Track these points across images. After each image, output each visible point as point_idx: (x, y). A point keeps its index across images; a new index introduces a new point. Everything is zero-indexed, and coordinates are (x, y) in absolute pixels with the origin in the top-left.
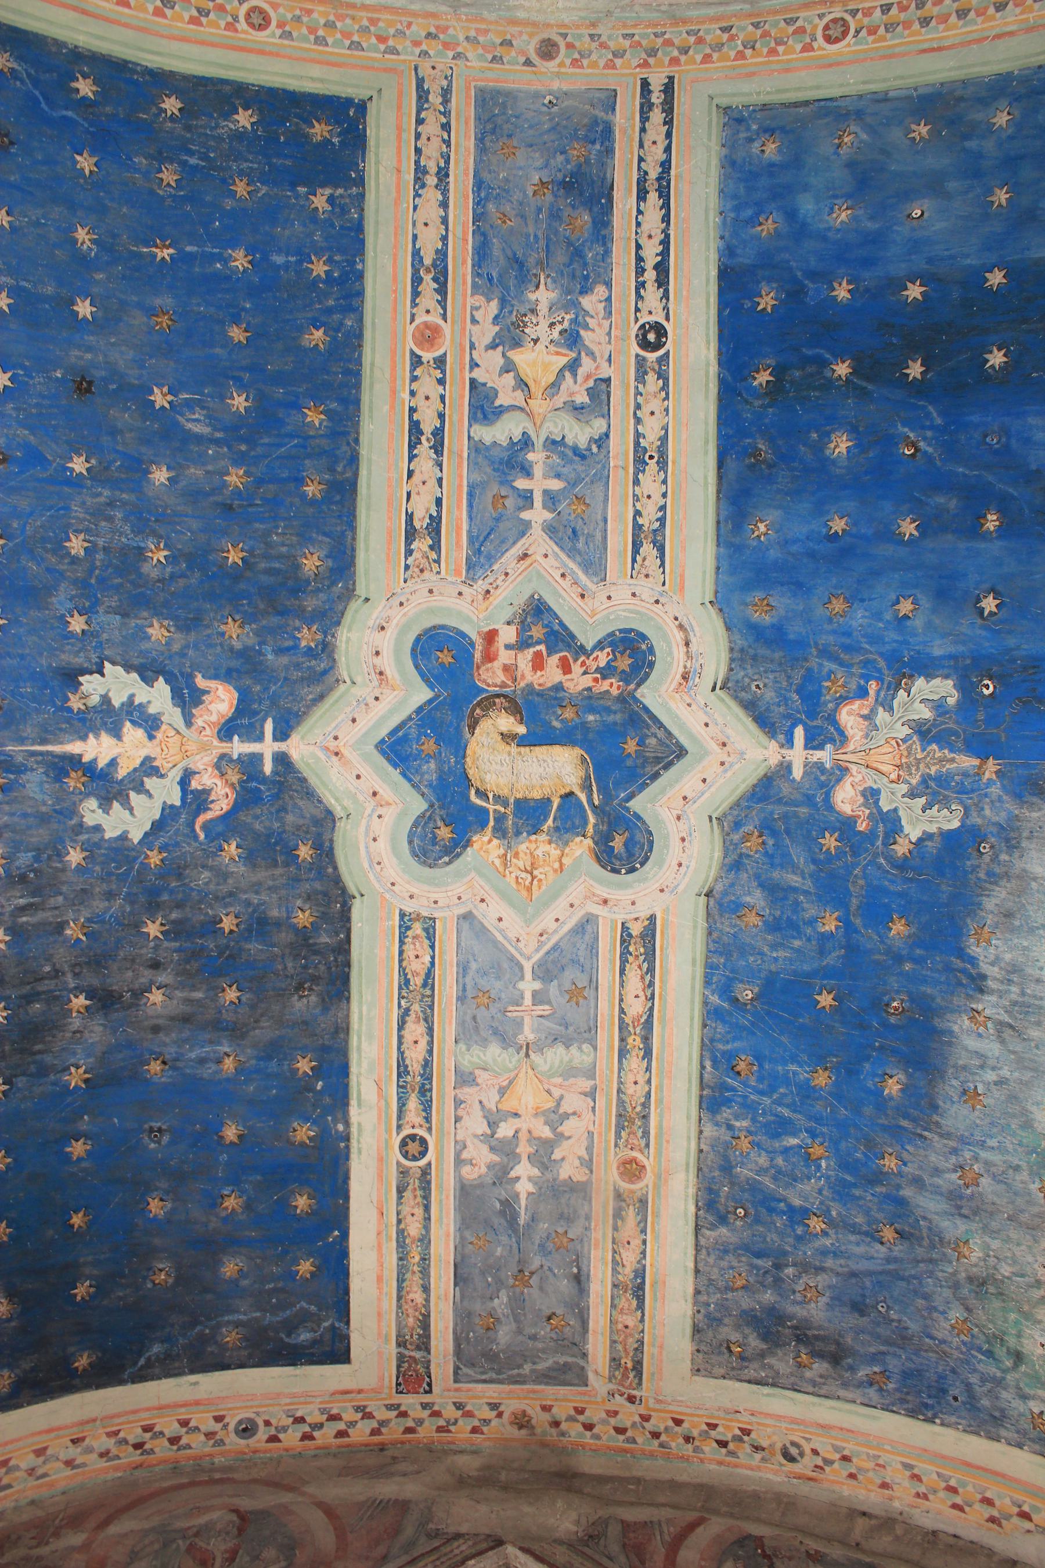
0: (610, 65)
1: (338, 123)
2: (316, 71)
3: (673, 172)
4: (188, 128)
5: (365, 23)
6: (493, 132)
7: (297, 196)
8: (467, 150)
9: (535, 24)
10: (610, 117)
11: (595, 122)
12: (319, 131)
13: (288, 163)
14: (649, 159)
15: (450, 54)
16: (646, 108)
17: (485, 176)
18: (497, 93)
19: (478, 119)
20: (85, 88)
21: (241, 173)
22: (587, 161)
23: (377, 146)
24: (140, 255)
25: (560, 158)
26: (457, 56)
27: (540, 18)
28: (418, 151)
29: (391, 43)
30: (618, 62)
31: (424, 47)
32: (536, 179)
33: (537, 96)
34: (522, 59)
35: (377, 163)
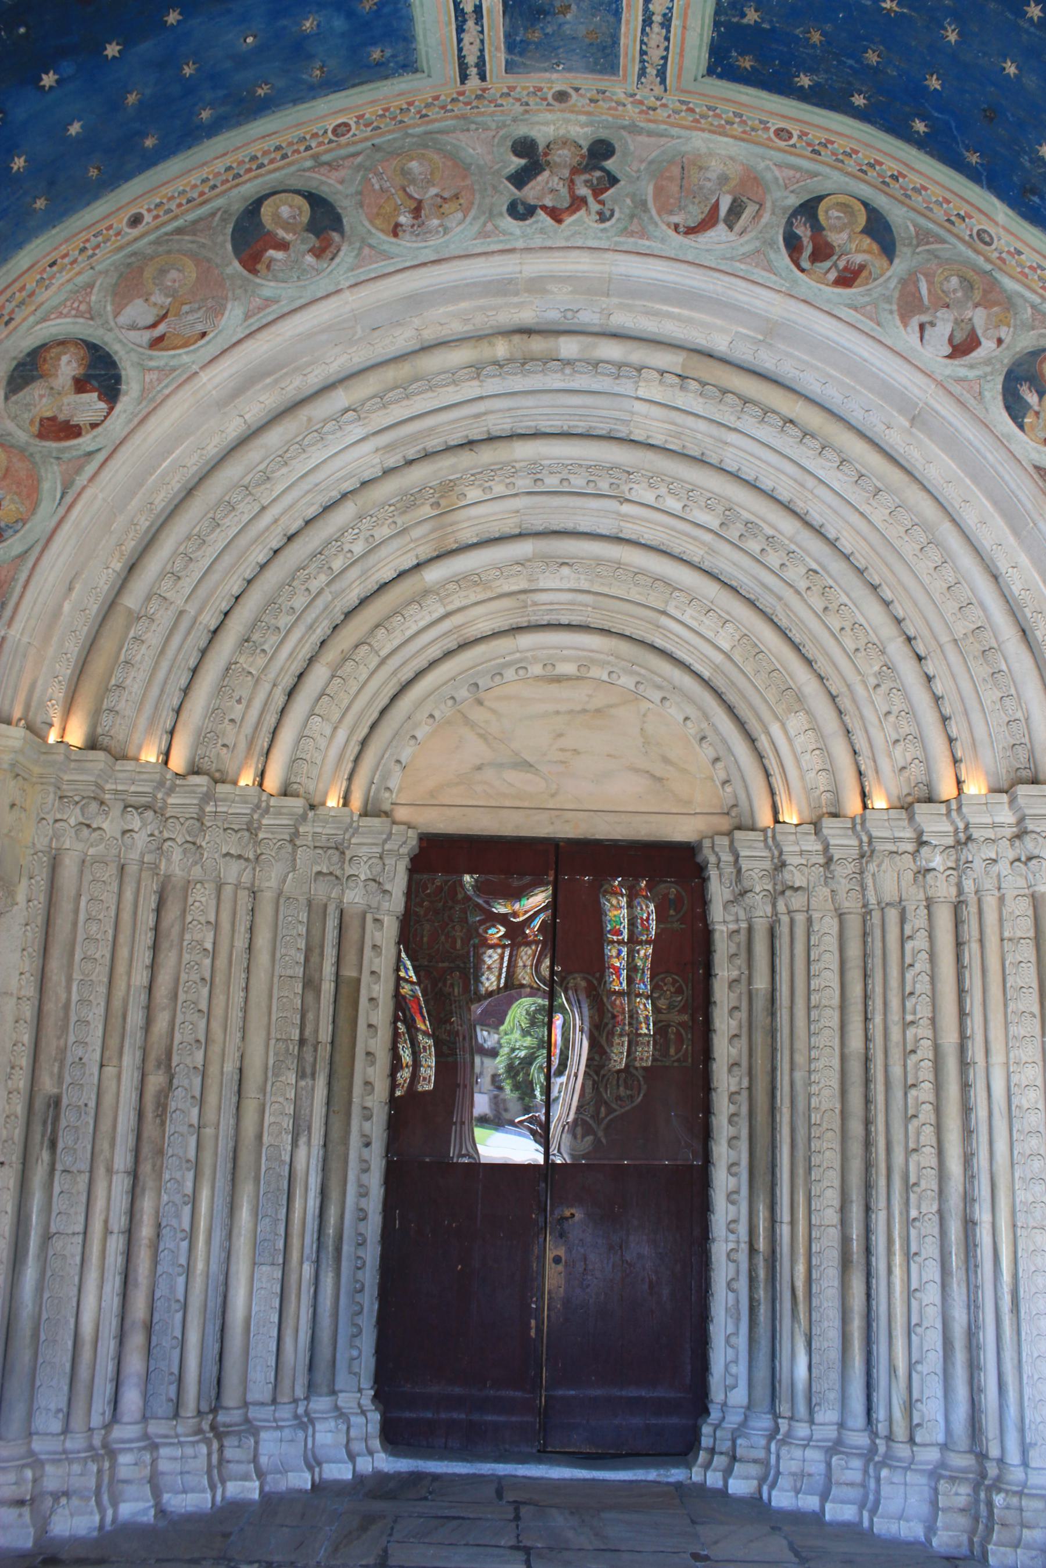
0: (512, 88)
1: (731, 65)
2: (743, 99)
3: (454, 26)
4: (850, 83)
5: (703, 121)
6: (605, 48)
7: (771, 22)
8: (627, 37)
9: (572, 112)
10: (509, 57)
11: (521, 54)
12: (747, 63)
13: (774, 46)
14: (475, 33)
15: (638, 97)
16: (481, 64)
17: (612, 19)
18: (602, 71)
19: (617, 57)
20: (920, 126)
21: (814, 46)
22: (526, 29)
23: (700, 46)
24: (910, 8)
25: (549, 30)
26: (633, 95)
27: (567, 115)
28: (667, 39)
29: (684, 107)
30: (505, 90)
31: (658, 103)
32: (569, 17)
33: (569, 70)
34: (581, 92)
35: (701, 35)
